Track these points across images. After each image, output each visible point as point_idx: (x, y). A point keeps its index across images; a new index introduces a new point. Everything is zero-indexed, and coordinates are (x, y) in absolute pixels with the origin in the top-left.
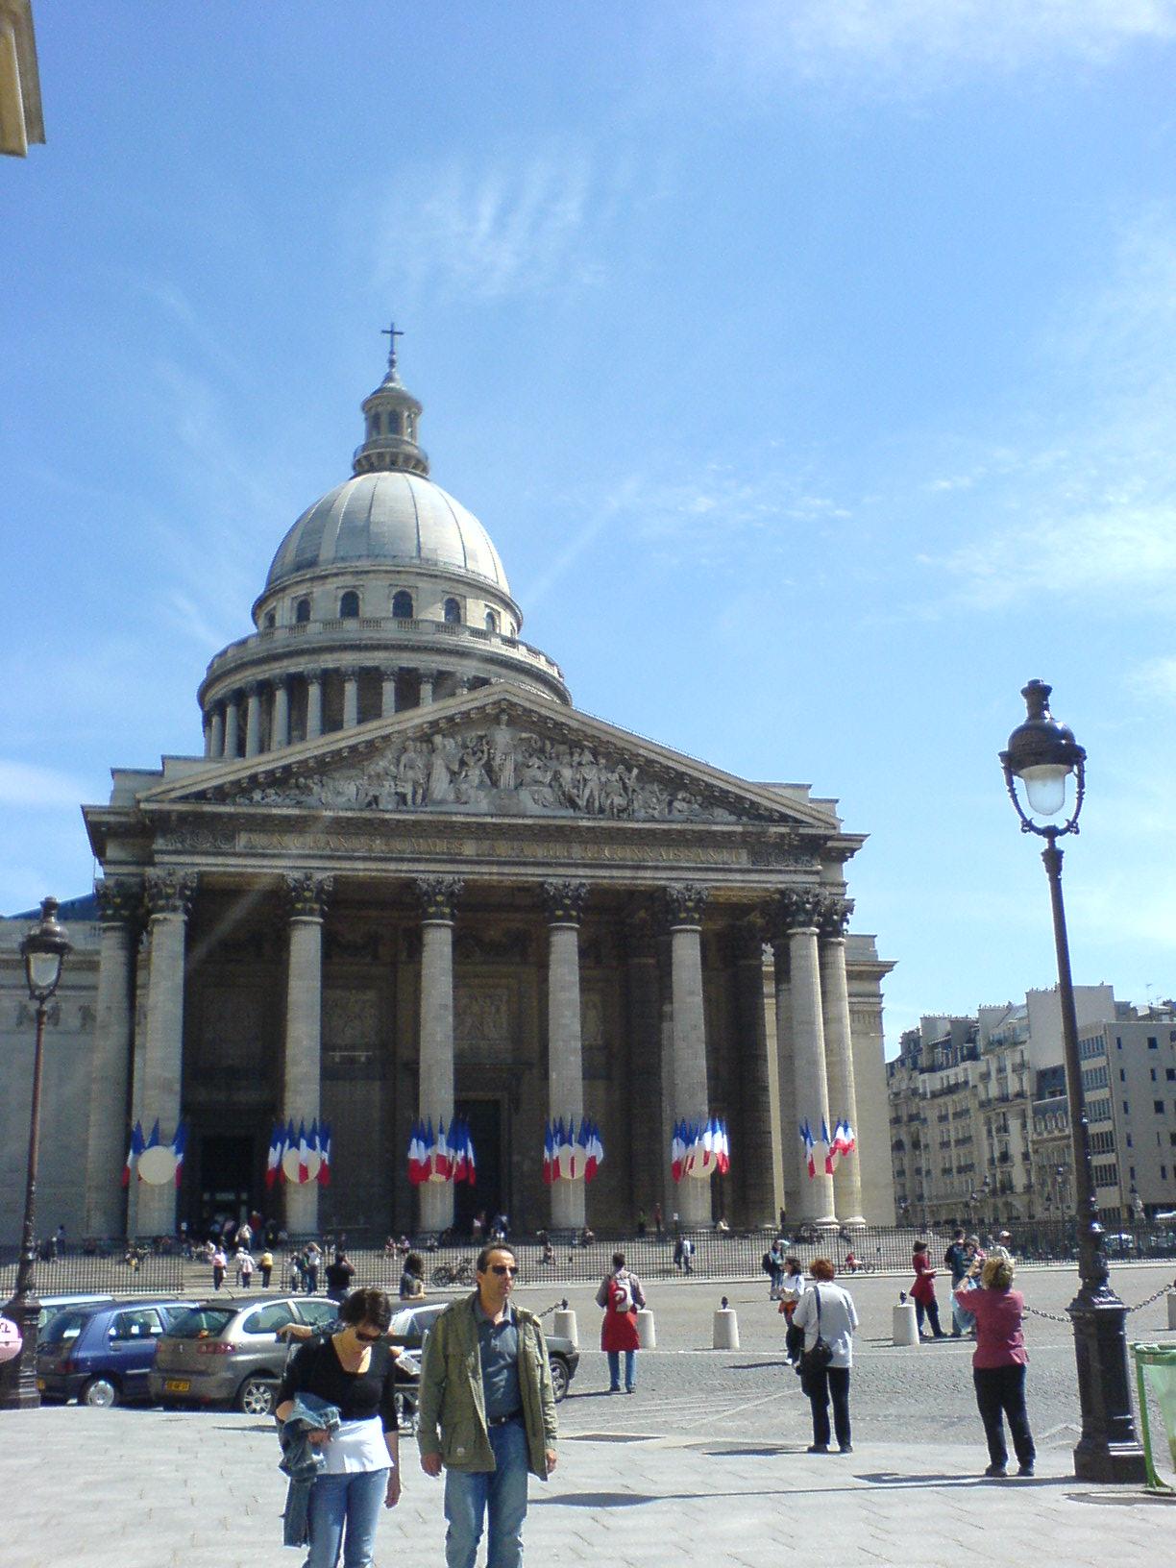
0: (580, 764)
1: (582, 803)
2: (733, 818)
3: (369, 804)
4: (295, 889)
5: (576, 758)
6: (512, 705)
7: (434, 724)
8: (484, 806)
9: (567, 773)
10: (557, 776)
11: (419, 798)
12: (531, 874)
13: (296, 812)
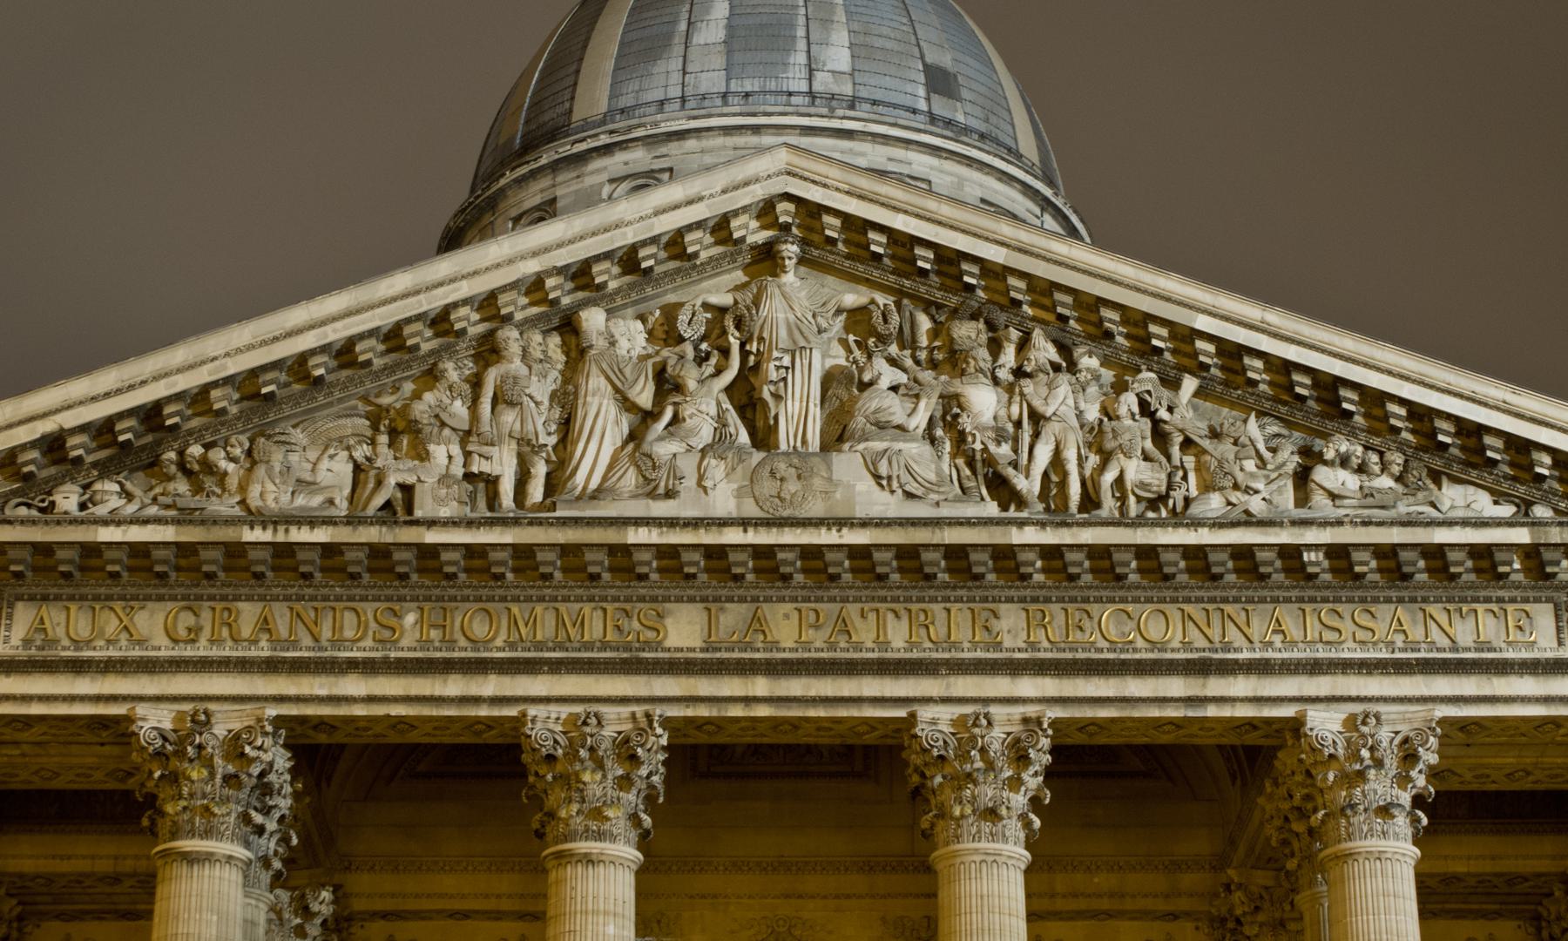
0: (1019, 373)
1: (1029, 485)
2: (1507, 511)
3: (388, 505)
4: (159, 754)
5: (1009, 357)
6: (811, 212)
7: (580, 275)
8: (723, 501)
9: (983, 402)
10: (951, 407)
11: (536, 492)
12: (870, 697)
13: (167, 534)
